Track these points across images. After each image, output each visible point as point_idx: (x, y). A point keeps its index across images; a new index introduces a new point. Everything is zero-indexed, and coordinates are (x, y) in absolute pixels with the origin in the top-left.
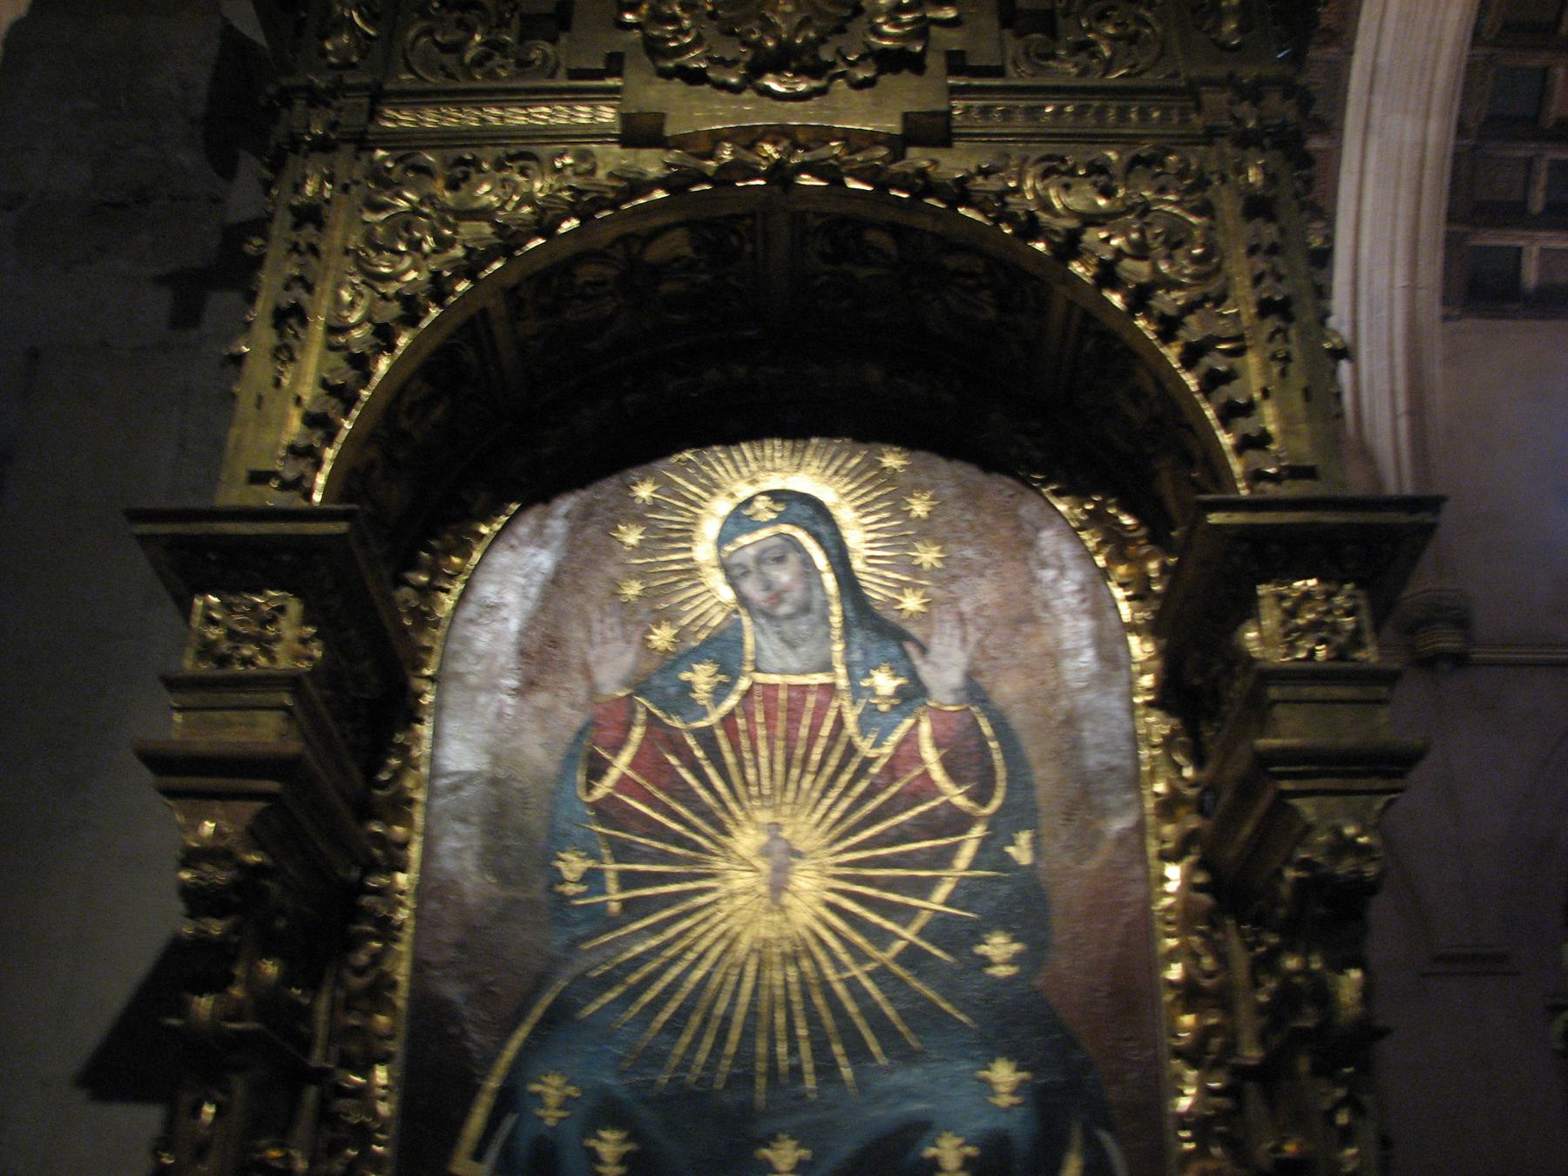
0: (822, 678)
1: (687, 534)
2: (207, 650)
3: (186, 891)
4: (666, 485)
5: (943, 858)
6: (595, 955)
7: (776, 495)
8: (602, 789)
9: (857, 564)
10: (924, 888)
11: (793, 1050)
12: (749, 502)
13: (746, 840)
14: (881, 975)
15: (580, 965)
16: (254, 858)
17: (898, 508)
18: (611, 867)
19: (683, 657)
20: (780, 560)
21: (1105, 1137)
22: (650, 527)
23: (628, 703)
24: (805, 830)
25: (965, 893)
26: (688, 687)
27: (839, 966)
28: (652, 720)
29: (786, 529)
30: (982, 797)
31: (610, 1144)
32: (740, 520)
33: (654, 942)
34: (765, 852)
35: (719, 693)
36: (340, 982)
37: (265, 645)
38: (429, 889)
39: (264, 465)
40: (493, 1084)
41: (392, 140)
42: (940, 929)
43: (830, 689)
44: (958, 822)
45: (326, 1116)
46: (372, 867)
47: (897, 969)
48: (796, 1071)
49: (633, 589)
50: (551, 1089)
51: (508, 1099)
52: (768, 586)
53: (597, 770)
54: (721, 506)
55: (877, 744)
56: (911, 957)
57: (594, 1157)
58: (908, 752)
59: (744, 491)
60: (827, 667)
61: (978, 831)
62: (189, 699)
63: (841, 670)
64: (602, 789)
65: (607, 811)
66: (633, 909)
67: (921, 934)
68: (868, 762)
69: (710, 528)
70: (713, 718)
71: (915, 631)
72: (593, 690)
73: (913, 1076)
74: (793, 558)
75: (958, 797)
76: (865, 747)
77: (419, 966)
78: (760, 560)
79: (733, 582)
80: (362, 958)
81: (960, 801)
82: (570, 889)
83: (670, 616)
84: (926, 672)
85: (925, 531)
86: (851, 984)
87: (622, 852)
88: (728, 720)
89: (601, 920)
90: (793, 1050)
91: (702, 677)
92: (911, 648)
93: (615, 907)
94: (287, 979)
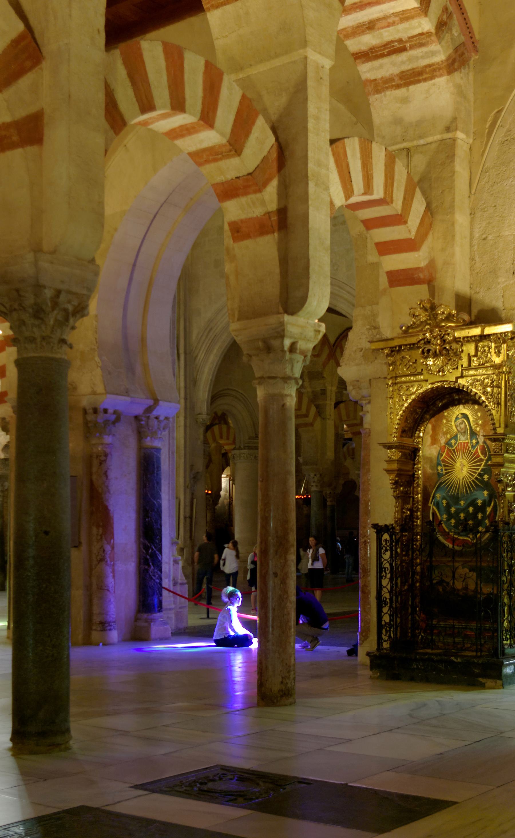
0: (467, 441)
1: (451, 420)
2: (389, 457)
3: (391, 483)
4: (448, 413)
5: (480, 465)
6: (443, 479)
7: (462, 414)
8: (442, 458)
9: (471, 424)
10: (478, 469)
11: (463, 490)
12: (458, 415)
13: (458, 464)
14: (473, 481)
15: (440, 481)
16: (397, 479)
17: (477, 415)
18: (444, 468)
19: (451, 439)
20: (462, 424)
21: (496, 500)
22: (447, 420)
23: (445, 446)
24: (465, 462)
25: (483, 470)
26: (452, 443)
27: (468, 480)
28: (448, 448)
29: (463, 419)
30: (485, 457)
31: (444, 502)
32: (457, 418)
33: (448, 477)
34: (460, 465)
35: (455, 444)
36: (413, 485)
37: (394, 456)
38: (424, 473)
39: (391, 434)
40: (432, 495)
41: (399, 383)
42: (480, 475)
43: (468, 443)
44: (482, 460)
45: (413, 501)
46: (416, 471)
47: (475, 480)
48: (464, 492)
49: (445, 429)
50: (438, 495)
51: (434, 497)
52: (461, 428)
53: (442, 455)
54: (455, 416)
55: (474, 450)
56: (476, 478)
57: (443, 503)
58: (477, 452)
59: (458, 413)
60: (468, 439)
61: (484, 461)
62: (388, 462)
63: (469, 440)
64: (442, 458)
65: (443, 461)
66: (446, 473)
67: (477, 475)
68: (472, 453)
69: (454, 419)
70: (454, 447)
71: (478, 434)
72: (441, 444)
73: (476, 492)
74: (463, 423)
75: (482, 457)
76: (472, 451)
77: (423, 482)
78: (460, 424)
79: (456, 427)
80: (415, 482)
81: (483, 458)
82: (439, 471)
83: (449, 433)
84: (479, 440)
85: (480, 418)
86: (470, 482)
87: (445, 466)
88: (456, 448)
89: (443, 475)
90: (463, 490)
91: (453, 442)
92: (477, 436)
93: (444, 473)
94: (403, 489)
